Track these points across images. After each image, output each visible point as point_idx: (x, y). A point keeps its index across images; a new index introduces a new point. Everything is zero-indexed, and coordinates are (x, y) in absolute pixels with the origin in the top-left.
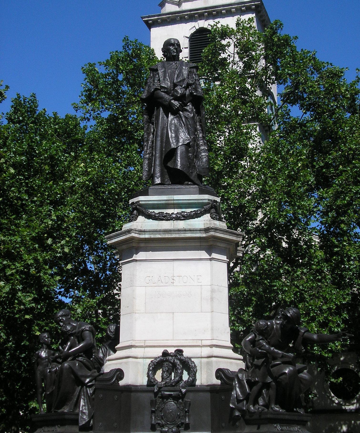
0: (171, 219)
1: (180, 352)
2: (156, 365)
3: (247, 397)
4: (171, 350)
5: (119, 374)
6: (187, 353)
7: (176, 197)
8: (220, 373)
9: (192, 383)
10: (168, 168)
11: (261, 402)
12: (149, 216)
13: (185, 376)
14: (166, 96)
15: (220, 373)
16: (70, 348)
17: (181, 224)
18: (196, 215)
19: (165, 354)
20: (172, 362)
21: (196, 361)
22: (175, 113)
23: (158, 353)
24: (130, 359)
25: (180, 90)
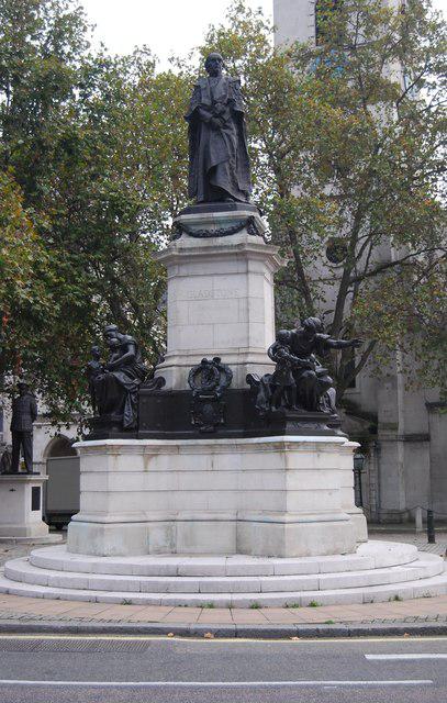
1: (217, 360)
3: (270, 401)
4: (210, 359)
5: (162, 381)
6: (224, 360)
8: (249, 378)
10: (212, 186)
11: (283, 404)
14: (208, 115)
16: (115, 359)
17: (220, 241)
19: (204, 362)
20: (210, 370)
21: (233, 368)
22: (216, 129)
23: (198, 361)
24: (173, 368)
25: (220, 107)
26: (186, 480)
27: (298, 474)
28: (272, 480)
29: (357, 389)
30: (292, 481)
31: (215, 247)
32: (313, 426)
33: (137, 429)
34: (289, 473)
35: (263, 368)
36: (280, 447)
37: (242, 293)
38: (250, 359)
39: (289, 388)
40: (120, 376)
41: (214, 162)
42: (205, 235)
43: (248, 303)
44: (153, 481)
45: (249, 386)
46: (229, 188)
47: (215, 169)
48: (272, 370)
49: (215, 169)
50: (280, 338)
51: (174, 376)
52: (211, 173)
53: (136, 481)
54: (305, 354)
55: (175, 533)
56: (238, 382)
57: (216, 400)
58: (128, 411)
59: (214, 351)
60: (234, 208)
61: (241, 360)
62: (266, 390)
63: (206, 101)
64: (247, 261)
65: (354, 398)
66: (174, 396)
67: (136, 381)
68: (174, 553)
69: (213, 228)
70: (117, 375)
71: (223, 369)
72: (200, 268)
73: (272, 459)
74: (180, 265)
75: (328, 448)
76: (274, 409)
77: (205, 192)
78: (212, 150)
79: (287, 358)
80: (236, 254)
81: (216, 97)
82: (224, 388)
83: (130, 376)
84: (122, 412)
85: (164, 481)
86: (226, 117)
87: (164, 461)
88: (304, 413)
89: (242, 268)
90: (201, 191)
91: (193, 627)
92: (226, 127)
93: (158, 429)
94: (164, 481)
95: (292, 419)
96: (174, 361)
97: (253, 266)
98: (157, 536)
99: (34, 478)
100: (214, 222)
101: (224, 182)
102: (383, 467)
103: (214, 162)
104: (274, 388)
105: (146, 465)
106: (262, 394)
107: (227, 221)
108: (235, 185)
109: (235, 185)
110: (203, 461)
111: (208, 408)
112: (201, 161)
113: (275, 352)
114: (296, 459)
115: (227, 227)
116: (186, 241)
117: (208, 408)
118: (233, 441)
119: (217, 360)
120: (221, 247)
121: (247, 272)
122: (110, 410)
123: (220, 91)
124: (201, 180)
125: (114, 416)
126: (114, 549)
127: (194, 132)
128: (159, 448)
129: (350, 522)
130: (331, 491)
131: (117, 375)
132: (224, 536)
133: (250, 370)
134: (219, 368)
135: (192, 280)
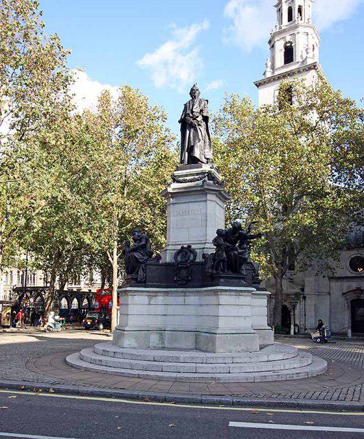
1: (189, 247)
2: (179, 252)
6: (193, 247)
8: (204, 256)
9: (193, 261)
11: (219, 269)
12: (178, 182)
13: (192, 258)
15: (204, 256)
20: (186, 251)
21: (197, 251)
23: (179, 247)
26: (171, 310)
32: (236, 281)
33: (145, 282)
39: (223, 261)
40: (137, 255)
42: (185, 181)
43: (206, 217)
44: (153, 309)
52: (191, 149)
53: (144, 310)
55: (165, 337)
56: (199, 259)
57: (187, 267)
58: (141, 272)
61: (202, 246)
64: (206, 194)
66: (167, 265)
68: (163, 348)
71: (193, 252)
76: (214, 272)
80: (200, 190)
82: (193, 261)
83: (142, 255)
85: (161, 310)
87: (160, 299)
88: (231, 274)
89: (204, 199)
93: (157, 282)
95: (223, 277)
97: (209, 197)
98: (154, 339)
105: (149, 302)
106: (209, 264)
107: (197, 174)
110: (180, 299)
113: (215, 241)
114: (224, 299)
118: (198, 289)
119: (189, 247)
120: (193, 187)
128: (157, 292)
129: (256, 335)
130: (245, 317)
132: (190, 343)
133: (206, 251)
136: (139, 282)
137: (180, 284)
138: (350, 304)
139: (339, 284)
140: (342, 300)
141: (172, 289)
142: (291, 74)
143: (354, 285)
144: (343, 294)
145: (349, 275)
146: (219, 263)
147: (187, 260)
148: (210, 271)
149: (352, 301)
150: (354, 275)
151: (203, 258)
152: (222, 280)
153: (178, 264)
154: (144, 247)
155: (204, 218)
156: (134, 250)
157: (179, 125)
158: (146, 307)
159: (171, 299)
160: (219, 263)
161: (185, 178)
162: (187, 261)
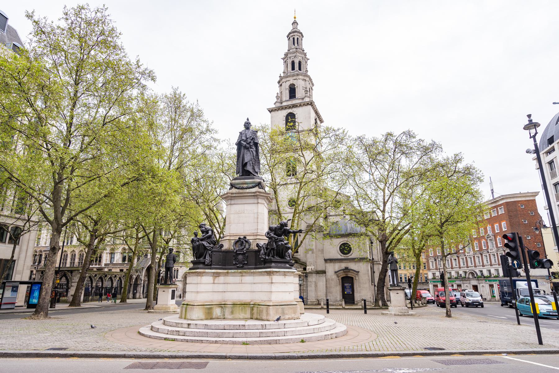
0: (244, 189)
1: (245, 237)
2: (236, 243)
3: (265, 254)
4: (242, 237)
5: (222, 246)
6: (248, 238)
7: (246, 181)
8: (258, 245)
12: (236, 188)
13: (247, 246)
14: (245, 143)
17: (248, 190)
18: (253, 187)
19: (239, 238)
20: (242, 241)
21: (251, 241)
22: (248, 149)
23: (237, 238)
25: (249, 140)
26: (230, 287)
27: (276, 285)
28: (266, 287)
29: (299, 254)
30: (274, 288)
31: (245, 193)
32: (283, 265)
33: (211, 265)
34: (273, 285)
35: (264, 241)
36: (269, 273)
37: (256, 211)
38: (258, 237)
39: (273, 249)
41: (246, 161)
45: (257, 248)
46: (251, 171)
47: (246, 163)
48: (266, 242)
49: (246, 163)
50: (271, 229)
51: (227, 246)
52: (244, 165)
53: (210, 287)
54: (280, 236)
56: (254, 247)
57: (244, 254)
58: (208, 258)
59: (244, 234)
60: (253, 178)
62: (264, 250)
63: (244, 138)
65: (298, 257)
66: (227, 252)
67: (212, 245)
69: (245, 186)
70: (204, 243)
72: (239, 201)
73: (266, 278)
74: (231, 200)
75: (288, 274)
76: (267, 258)
77: (242, 172)
78: (245, 156)
79: (273, 237)
81: (248, 137)
82: (247, 249)
84: (205, 258)
85: (221, 288)
86: (251, 144)
87: (221, 279)
88: (277, 259)
89: (256, 201)
90: (241, 170)
91: (228, 355)
92: (251, 148)
93: (220, 265)
94: (221, 288)
96: (228, 238)
97: (260, 201)
99: (173, 286)
100: (245, 184)
101: (249, 168)
102: (309, 283)
103: (246, 161)
104: (267, 249)
105: (214, 281)
106: (262, 251)
107: (251, 183)
108: (254, 169)
109: (254, 169)
110: (237, 279)
111: (240, 257)
112: (241, 159)
114: (276, 278)
115: (251, 185)
116: (234, 190)
117: (240, 257)
120: (248, 193)
121: (258, 203)
122: (200, 257)
123: (249, 134)
124: (241, 168)
125: (201, 259)
126: (198, 317)
127: (239, 150)
130: (290, 292)
131: (204, 243)
133: (258, 242)
134: (246, 241)
135: (237, 206)
136: (207, 265)
137: (238, 267)
138: (341, 281)
139: (332, 264)
140: (334, 277)
141: (233, 271)
142: (294, 106)
143: (343, 265)
144: (336, 272)
145: (340, 257)
146: (270, 251)
147: (243, 249)
148: (263, 256)
149: (342, 278)
150: (343, 258)
151: (257, 246)
152: (273, 264)
153: (237, 251)
154: (210, 237)
155: (256, 216)
156: (202, 240)
157: (236, 147)
158: (212, 285)
159: (230, 279)
160: (270, 251)
161: (242, 186)
162: (243, 249)
